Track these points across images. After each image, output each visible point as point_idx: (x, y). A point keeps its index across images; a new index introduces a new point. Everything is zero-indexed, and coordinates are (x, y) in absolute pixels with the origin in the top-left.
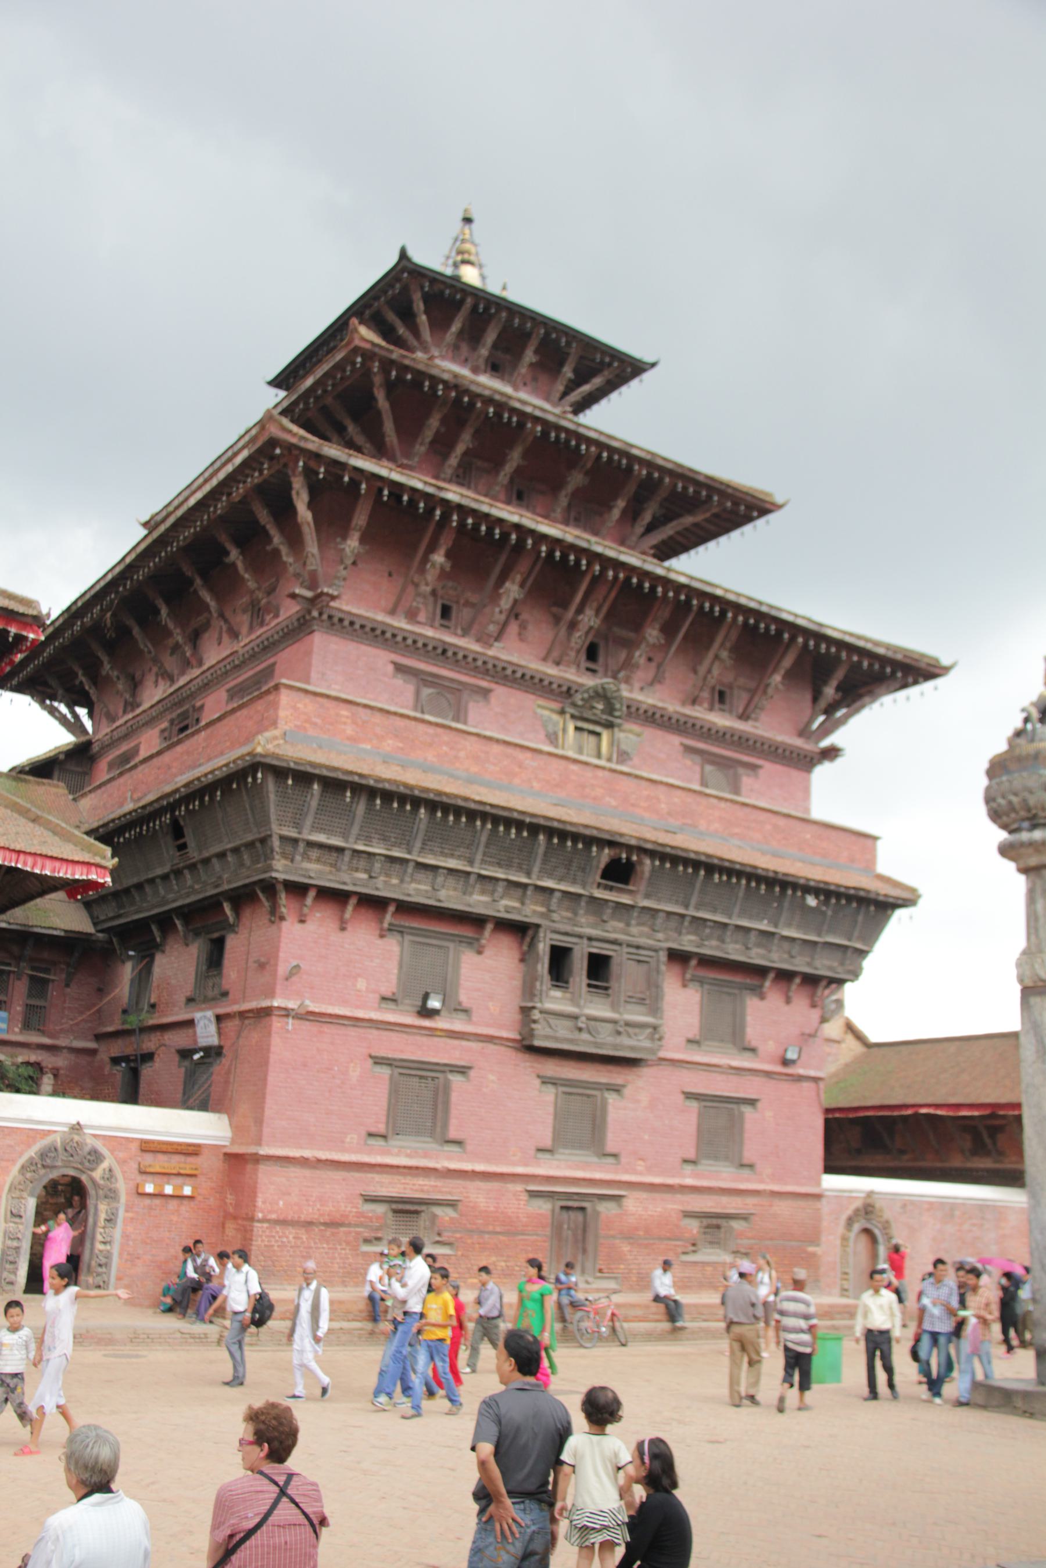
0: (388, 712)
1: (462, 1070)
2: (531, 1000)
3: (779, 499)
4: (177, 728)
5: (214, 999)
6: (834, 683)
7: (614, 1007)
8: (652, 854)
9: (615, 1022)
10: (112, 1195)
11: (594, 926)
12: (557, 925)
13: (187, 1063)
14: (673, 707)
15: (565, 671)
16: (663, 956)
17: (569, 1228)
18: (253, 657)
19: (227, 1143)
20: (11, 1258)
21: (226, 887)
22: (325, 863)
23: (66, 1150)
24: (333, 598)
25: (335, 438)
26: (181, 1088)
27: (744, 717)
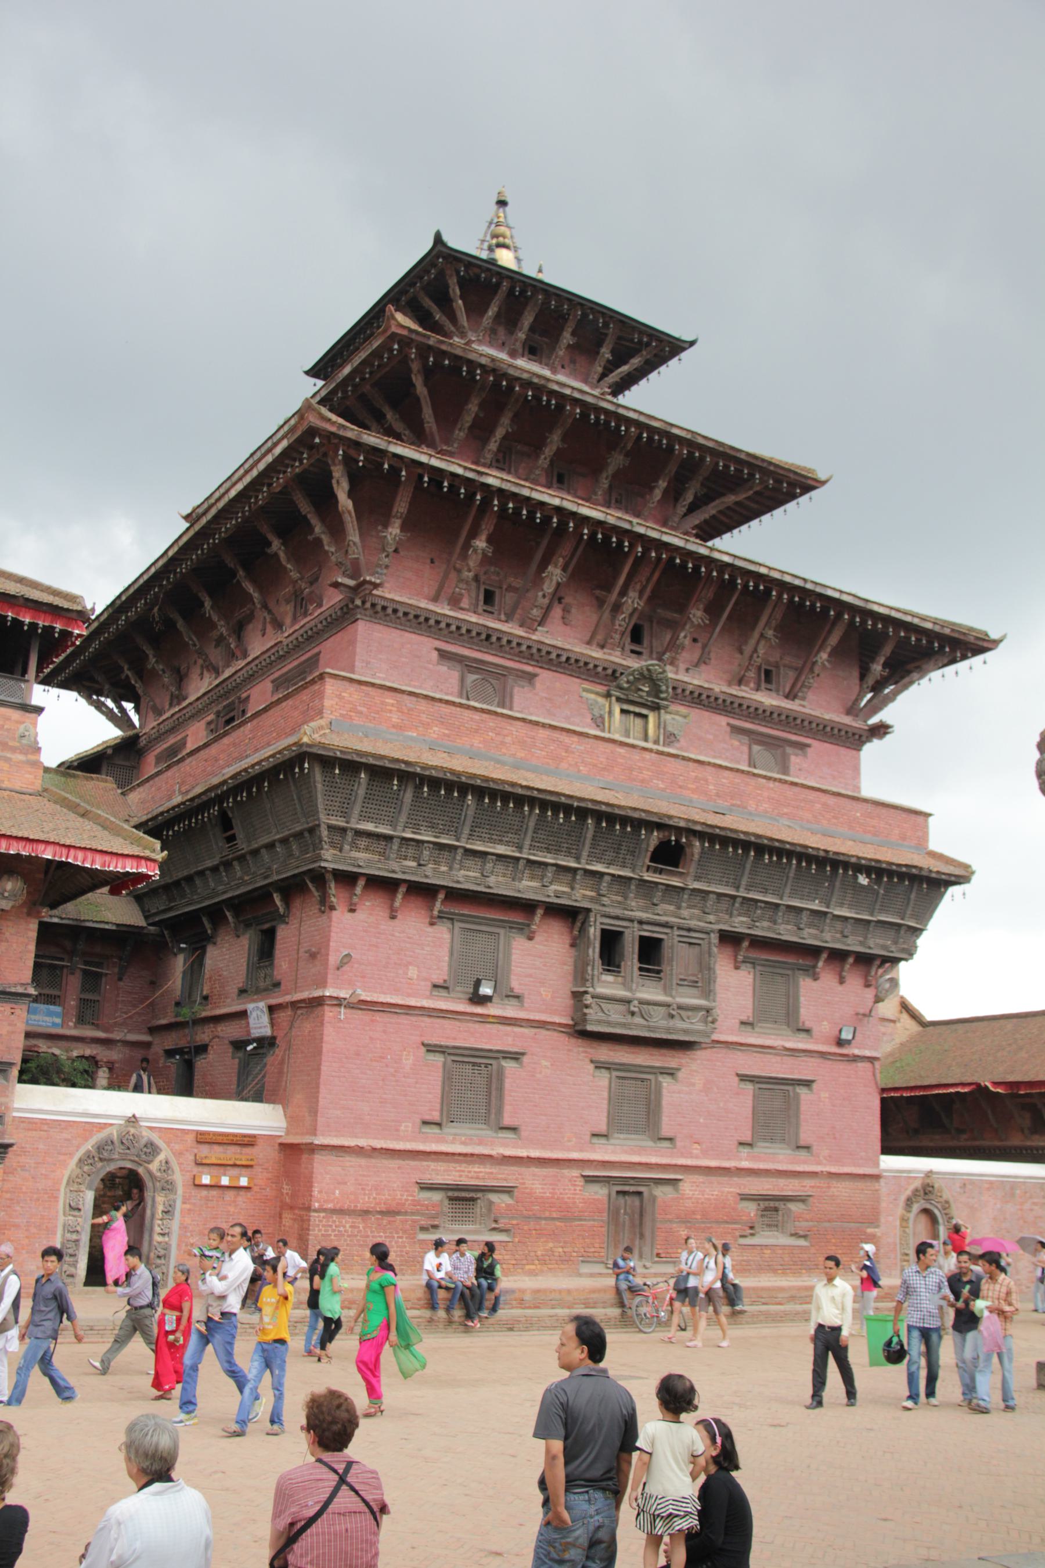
0: (433, 699)
1: (516, 1057)
2: (584, 985)
3: (822, 476)
4: (224, 719)
5: (266, 990)
6: (882, 660)
7: (666, 990)
8: (701, 835)
9: (668, 1005)
10: (169, 1187)
11: (644, 909)
12: (607, 908)
13: (240, 1054)
14: (719, 687)
15: (610, 654)
16: (714, 938)
17: (625, 1213)
18: (297, 647)
19: (282, 1134)
20: (70, 1251)
21: (275, 878)
22: (373, 852)
24: (376, 586)
25: (374, 425)
26: (235, 1079)
27: (791, 696)
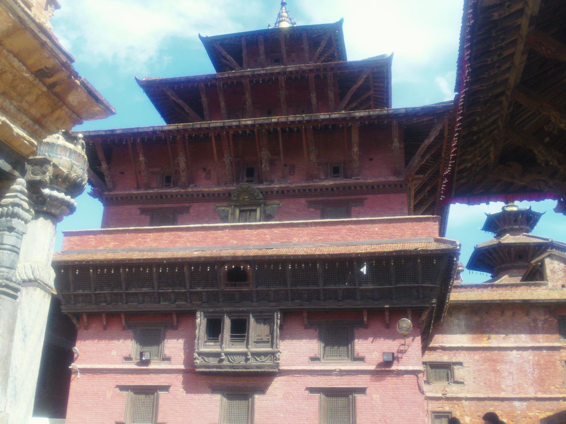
15: (230, 186)
27: (346, 177)
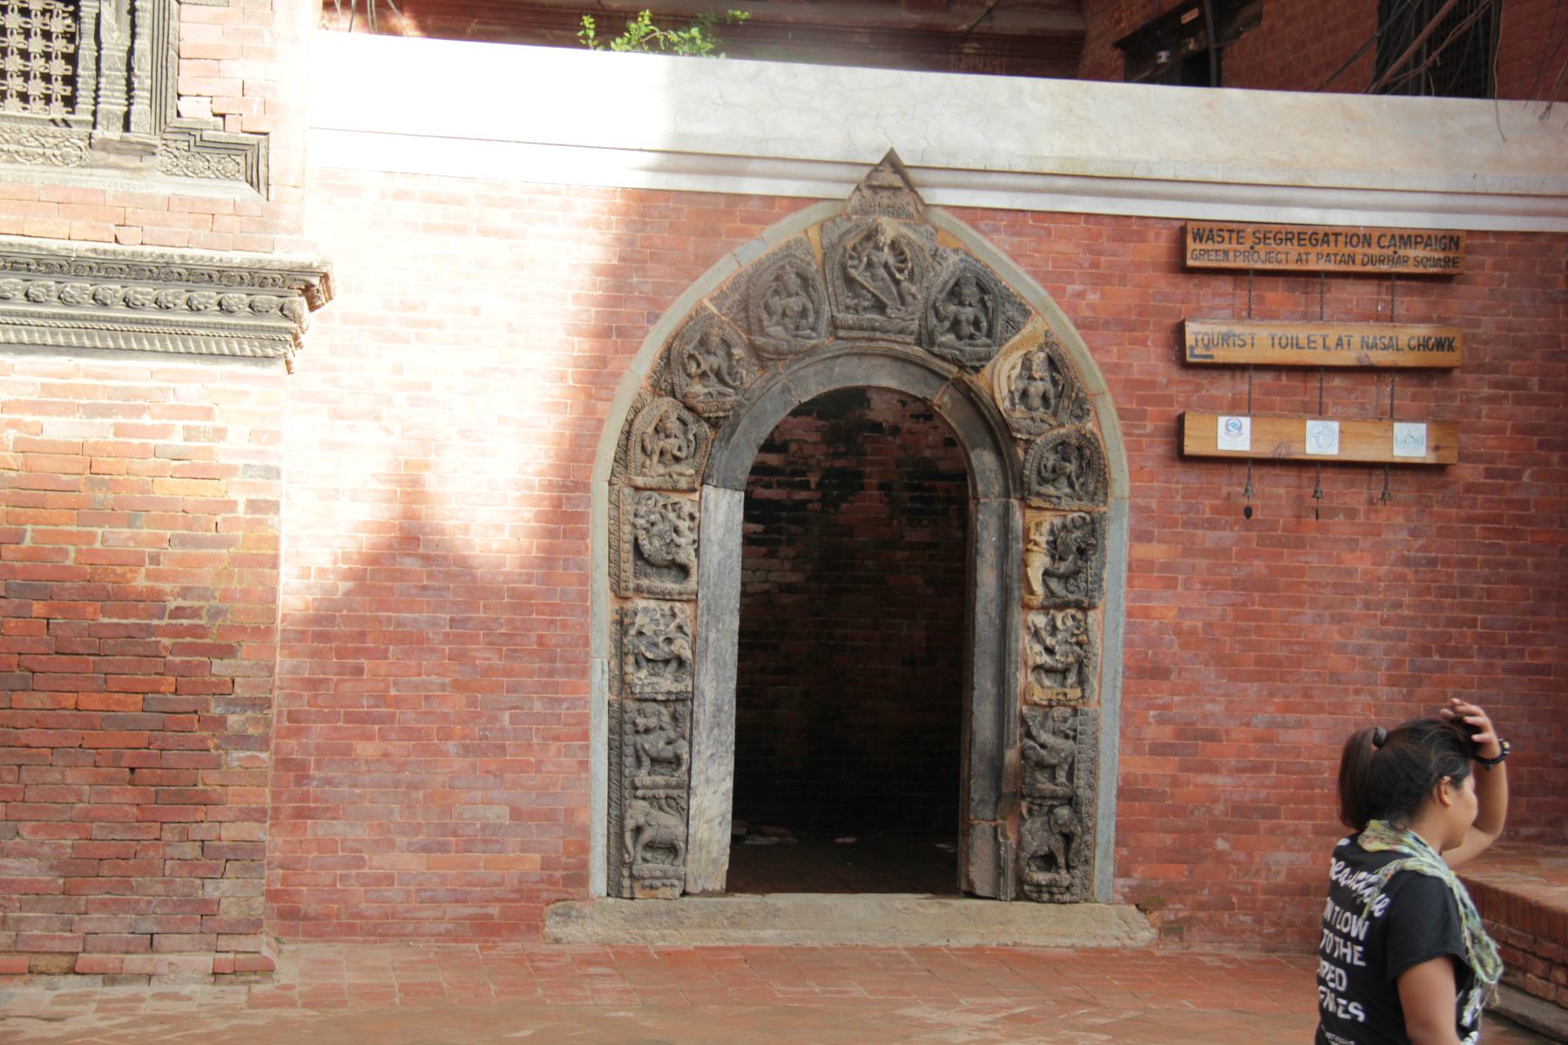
20: (655, 744)
23: (850, 282)
